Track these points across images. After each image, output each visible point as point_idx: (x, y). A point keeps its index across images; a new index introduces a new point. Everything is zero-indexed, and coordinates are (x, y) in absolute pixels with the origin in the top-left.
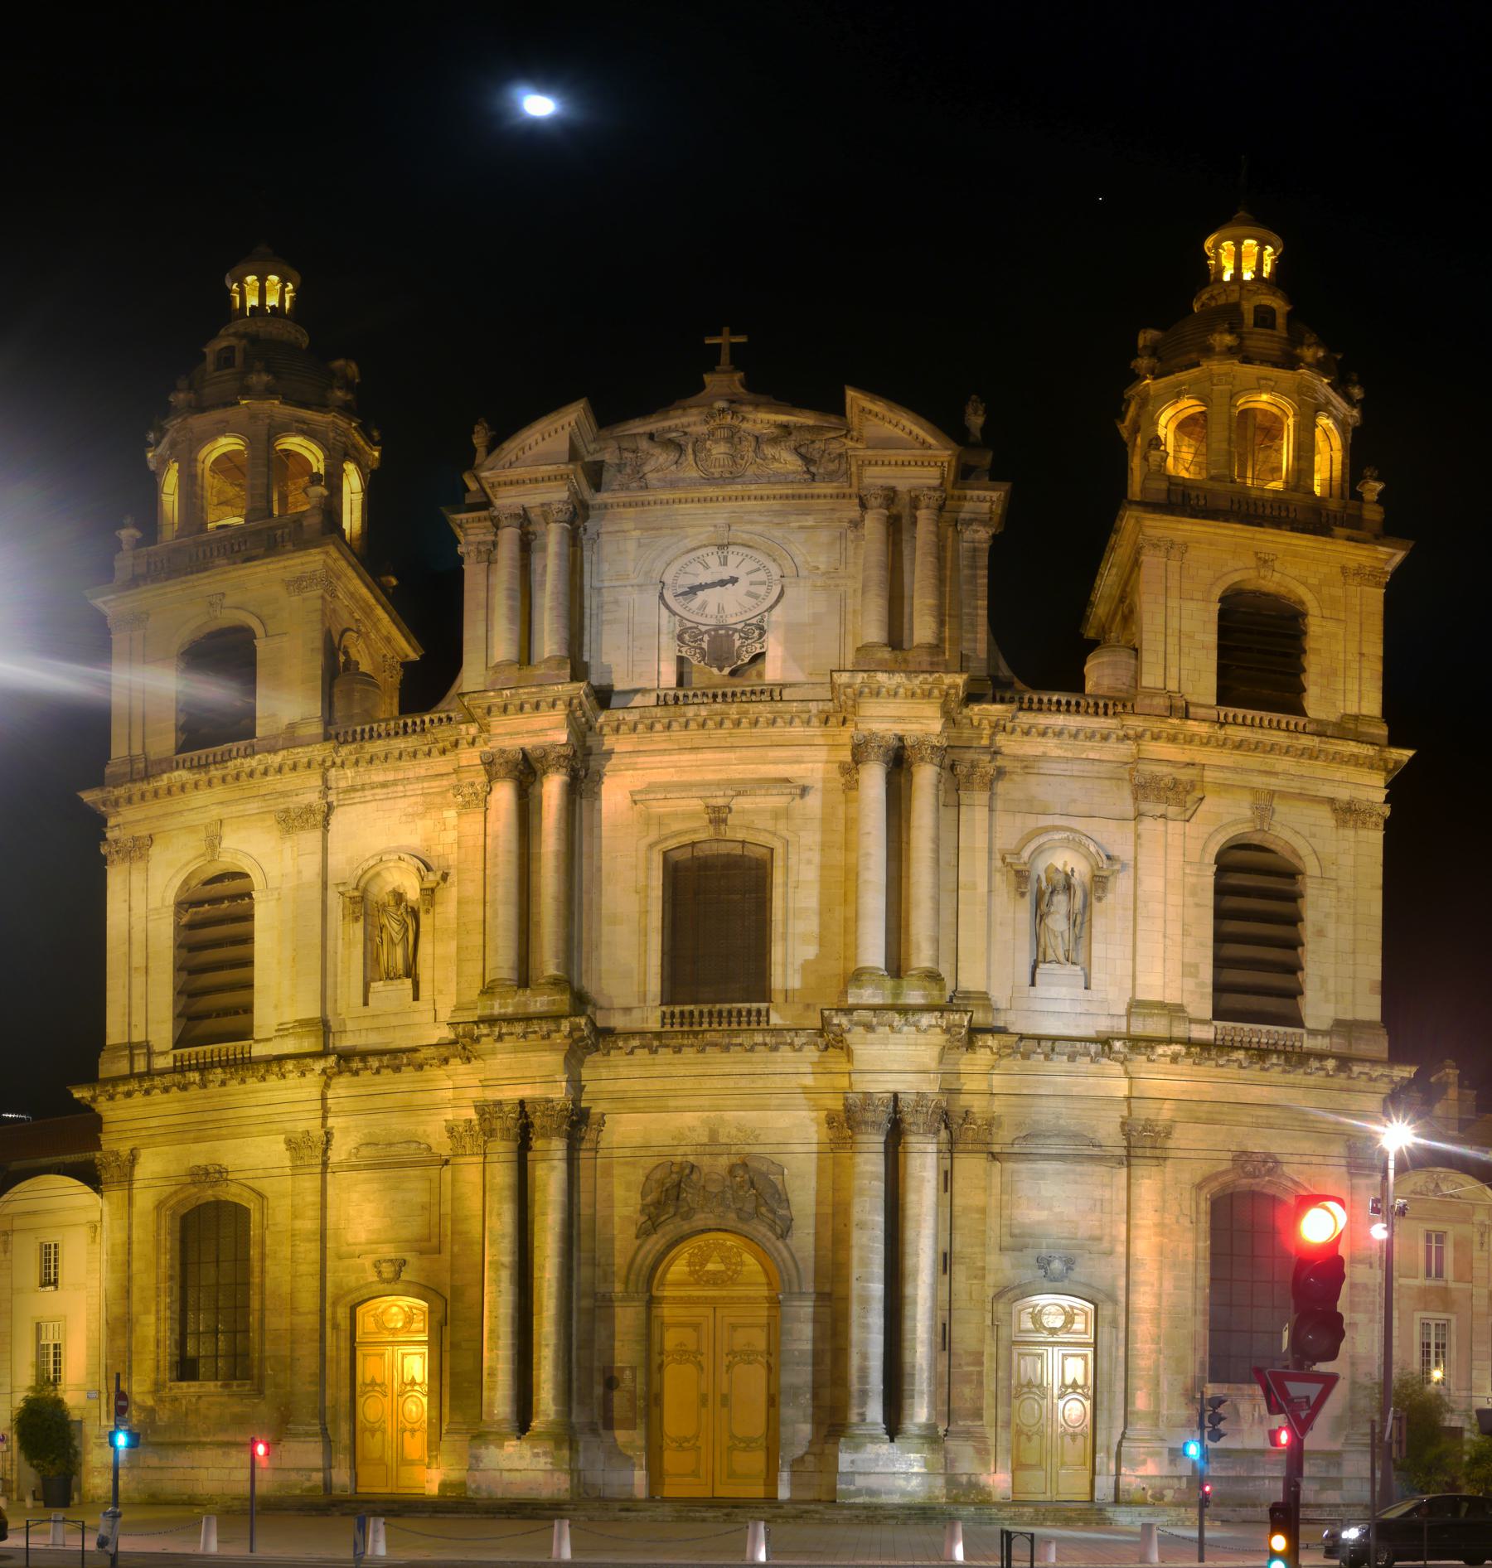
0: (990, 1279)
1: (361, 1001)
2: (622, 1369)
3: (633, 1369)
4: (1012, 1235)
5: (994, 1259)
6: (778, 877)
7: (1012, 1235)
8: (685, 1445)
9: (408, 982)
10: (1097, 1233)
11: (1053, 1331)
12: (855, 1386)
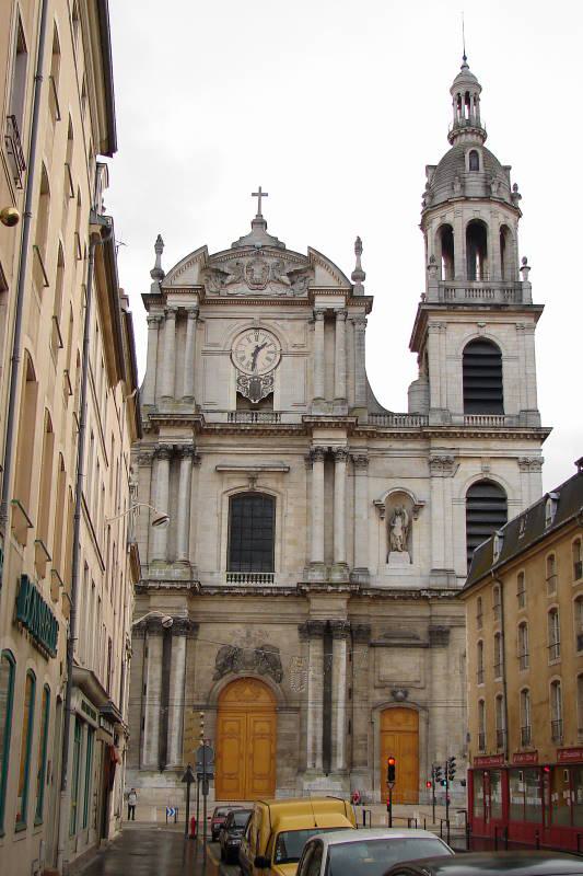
5: (372, 691)
10: (418, 679)
11: (399, 724)
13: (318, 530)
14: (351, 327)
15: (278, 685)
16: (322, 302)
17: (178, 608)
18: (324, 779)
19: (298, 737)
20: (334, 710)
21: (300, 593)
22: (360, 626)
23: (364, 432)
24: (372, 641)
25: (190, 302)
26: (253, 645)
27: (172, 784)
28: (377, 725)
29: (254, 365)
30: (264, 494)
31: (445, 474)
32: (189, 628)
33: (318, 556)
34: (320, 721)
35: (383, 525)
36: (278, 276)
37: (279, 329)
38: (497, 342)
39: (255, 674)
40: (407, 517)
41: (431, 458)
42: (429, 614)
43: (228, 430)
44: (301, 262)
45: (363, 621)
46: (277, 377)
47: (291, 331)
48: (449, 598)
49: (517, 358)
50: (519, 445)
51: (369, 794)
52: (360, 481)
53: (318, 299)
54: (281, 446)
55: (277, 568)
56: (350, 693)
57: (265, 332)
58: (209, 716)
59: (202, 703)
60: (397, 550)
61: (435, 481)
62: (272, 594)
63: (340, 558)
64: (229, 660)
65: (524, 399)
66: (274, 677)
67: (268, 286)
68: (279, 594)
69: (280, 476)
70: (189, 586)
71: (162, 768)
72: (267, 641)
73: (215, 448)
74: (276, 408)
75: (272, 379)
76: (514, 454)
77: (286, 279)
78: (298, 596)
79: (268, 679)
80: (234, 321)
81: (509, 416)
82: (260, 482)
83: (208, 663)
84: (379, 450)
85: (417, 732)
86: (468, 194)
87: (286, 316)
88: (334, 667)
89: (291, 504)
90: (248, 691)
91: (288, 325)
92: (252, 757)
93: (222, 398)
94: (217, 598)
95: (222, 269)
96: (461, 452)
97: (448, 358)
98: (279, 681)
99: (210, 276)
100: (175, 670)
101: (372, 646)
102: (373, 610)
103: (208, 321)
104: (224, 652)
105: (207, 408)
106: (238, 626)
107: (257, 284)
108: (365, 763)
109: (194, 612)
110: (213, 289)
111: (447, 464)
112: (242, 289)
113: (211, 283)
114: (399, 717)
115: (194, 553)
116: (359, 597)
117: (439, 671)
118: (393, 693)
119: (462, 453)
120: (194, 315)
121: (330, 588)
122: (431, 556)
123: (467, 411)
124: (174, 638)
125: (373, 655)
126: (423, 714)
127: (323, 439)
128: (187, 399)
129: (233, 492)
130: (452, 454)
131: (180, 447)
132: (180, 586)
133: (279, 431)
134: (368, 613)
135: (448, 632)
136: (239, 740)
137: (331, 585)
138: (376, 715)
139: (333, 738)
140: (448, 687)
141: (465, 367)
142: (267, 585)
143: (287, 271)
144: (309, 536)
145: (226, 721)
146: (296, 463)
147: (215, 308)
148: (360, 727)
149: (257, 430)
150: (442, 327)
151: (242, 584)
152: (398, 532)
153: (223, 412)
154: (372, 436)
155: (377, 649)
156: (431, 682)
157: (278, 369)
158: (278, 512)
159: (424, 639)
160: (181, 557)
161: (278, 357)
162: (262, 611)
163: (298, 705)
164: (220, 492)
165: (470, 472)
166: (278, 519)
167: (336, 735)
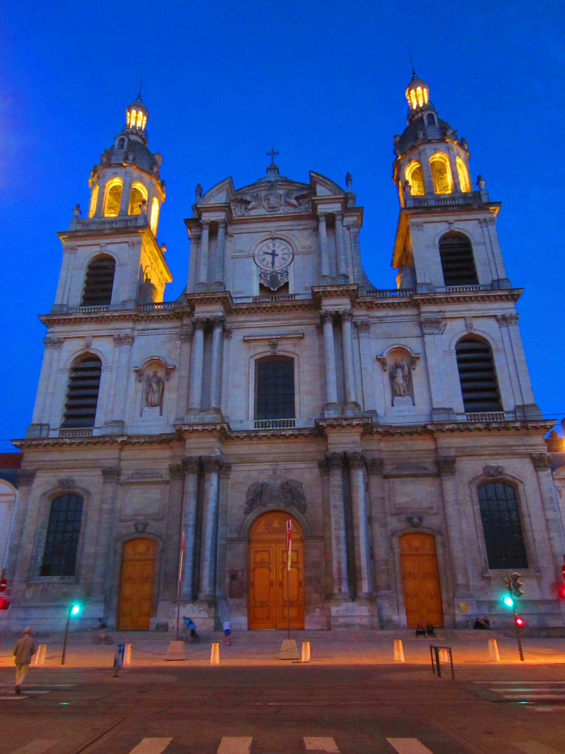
0: (389, 527)
1: (139, 414)
2: (237, 571)
3: (242, 571)
4: (396, 509)
5: (389, 519)
6: (296, 364)
7: (396, 509)
8: (264, 604)
9: (158, 409)
10: (431, 505)
11: (417, 549)
12: (335, 576)
13: (332, 377)
14: (347, 232)
15: (302, 516)
16: (322, 209)
17: (210, 448)
18: (350, 604)
19: (323, 565)
20: (356, 534)
21: (319, 432)
22: (374, 459)
23: (365, 303)
24: (386, 473)
25: (219, 216)
26: (279, 482)
27: (204, 614)
28: (397, 551)
29: (273, 263)
30: (283, 356)
31: (435, 332)
32: (222, 467)
33: (333, 398)
34: (343, 547)
35: (386, 377)
36: (288, 200)
37: (291, 237)
38: (466, 233)
39: (282, 506)
40: (406, 368)
41: (422, 319)
42: (432, 447)
43: (253, 309)
44: (306, 189)
45: (376, 455)
46: (291, 271)
47: (302, 239)
48: (452, 430)
49: (484, 243)
50: (496, 305)
51: (395, 618)
52: (363, 341)
53: (319, 207)
54: (294, 318)
55: (297, 415)
56: (369, 520)
57: (282, 241)
58: (241, 547)
59: (235, 535)
60: (401, 396)
61: (427, 338)
62: (293, 435)
63: (352, 398)
64: (257, 495)
65: (494, 272)
66: (298, 509)
67: (281, 208)
68: (300, 435)
69: (296, 341)
70: (218, 427)
71: (194, 597)
72: (292, 476)
73: (242, 324)
74: (291, 291)
75: (287, 272)
76: (492, 313)
77: (294, 202)
78: (316, 436)
79: (294, 511)
80: (256, 234)
81: (484, 286)
82: (279, 348)
83: (237, 499)
84: (376, 317)
85: (435, 555)
86: (430, 138)
87: (295, 228)
88: (354, 494)
89: (307, 363)
90: (276, 524)
91: (297, 233)
92: (281, 584)
93: (246, 285)
94: (246, 440)
95: (245, 199)
96: (446, 314)
97: (427, 247)
98: (303, 512)
99: (236, 206)
100: (207, 503)
101: (386, 477)
102: (382, 445)
103: (235, 236)
104: (253, 488)
105: (236, 296)
106: (265, 466)
107: (272, 208)
108: (389, 588)
109: (225, 455)
110: (240, 214)
111: (436, 323)
112: (262, 212)
113: (238, 210)
114: (416, 542)
115: (227, 406)
116: (371, 433)
117: (450, 497)
118: (409, 520)
119: (448, 315)
120: (223, 225)
121: (344, 423)
122: (431, 399)
123: (447, 284)
124: (207, 475)
125: (387, 486)
126: (439, 539)
127: (330, 305)
128: (218, 284)
129: (258, 357)
130: (439, 316)
131: (212, 319)
132: (210, 428)
133: (294, 306)
134: (381, 447)
135: (454, 462)
136: (270, 570)
137: (346, 419)
138: (395, 540)
139: (357, 562)
140: (459, 512)
141: (442, 255)
142: (289, 428)
143: (295, 195)
144: (324, 387)
145: (256, 552)
146: (309, 330)
147: (240, 226)
148: (381, 552)
149: (276, 307)
150: (419, 226)
151: (267, 428)
152: (400, 380)
153: (248, 297)
154: (370, 306)
155: (391, 480)
156: (444, 508)
157: (292, 265)
158: (296, 370)
159: (432, 469)
160: (214, 405)
161: (291, 256)
162: (286, 450)
163: (322, 534)
164: (248, 356)
165: (455, 330)
166: (296, 376)
167: (360, 559)
